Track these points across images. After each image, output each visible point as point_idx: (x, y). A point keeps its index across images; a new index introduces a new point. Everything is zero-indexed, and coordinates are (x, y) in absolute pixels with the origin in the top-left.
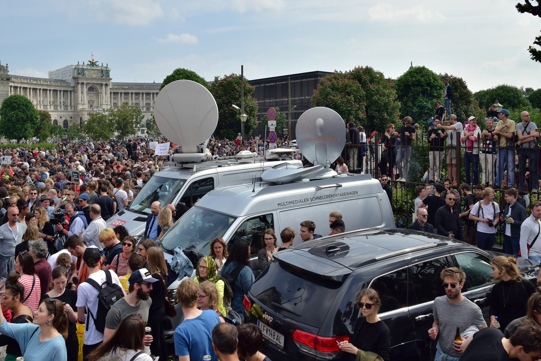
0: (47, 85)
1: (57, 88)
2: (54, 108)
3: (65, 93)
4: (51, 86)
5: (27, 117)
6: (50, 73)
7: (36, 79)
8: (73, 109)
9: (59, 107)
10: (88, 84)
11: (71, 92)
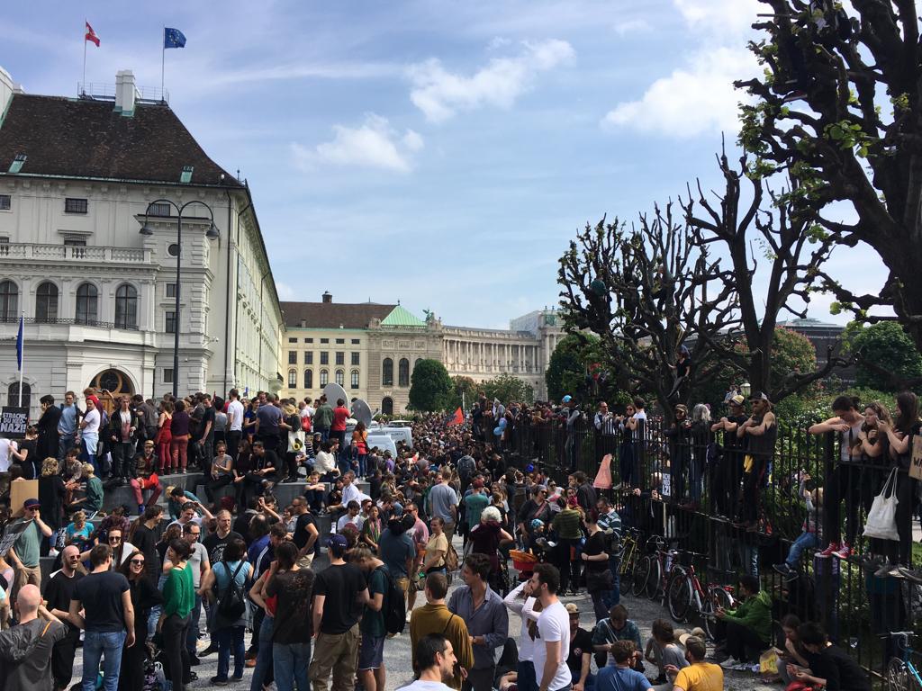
0: (505, 339)
1: (518, 343)
2: (514, 370)
3: (529, 350)
4: (510, 340)
5: (439, 385)
6: (513, 323)
7: (490, 332)
9: (520, 369)
11: (536, 347)
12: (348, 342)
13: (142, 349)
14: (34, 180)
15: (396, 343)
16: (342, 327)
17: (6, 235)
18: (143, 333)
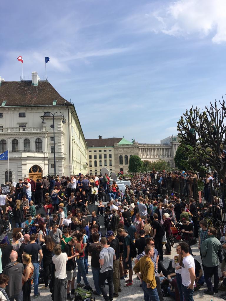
1: (164, 148)
4: (161, 147)
6: (161, 141)
7: (153, 145)
8: (171, 157)
9: (165, 156)
10: (177, 145)
11: (170, 149)
12: (108, 151)
13: (44, 159)
14: (10, 108)
15: (123, 151)
16: (105, 146)
17: (2, 126)
18: (44, 153)
